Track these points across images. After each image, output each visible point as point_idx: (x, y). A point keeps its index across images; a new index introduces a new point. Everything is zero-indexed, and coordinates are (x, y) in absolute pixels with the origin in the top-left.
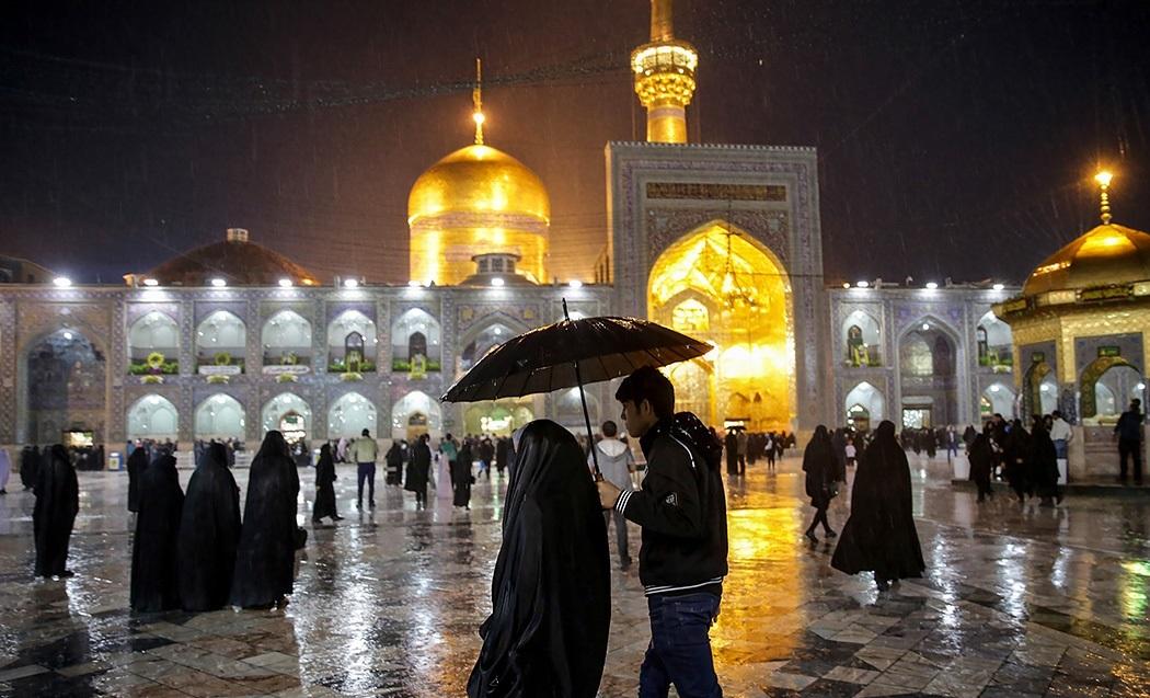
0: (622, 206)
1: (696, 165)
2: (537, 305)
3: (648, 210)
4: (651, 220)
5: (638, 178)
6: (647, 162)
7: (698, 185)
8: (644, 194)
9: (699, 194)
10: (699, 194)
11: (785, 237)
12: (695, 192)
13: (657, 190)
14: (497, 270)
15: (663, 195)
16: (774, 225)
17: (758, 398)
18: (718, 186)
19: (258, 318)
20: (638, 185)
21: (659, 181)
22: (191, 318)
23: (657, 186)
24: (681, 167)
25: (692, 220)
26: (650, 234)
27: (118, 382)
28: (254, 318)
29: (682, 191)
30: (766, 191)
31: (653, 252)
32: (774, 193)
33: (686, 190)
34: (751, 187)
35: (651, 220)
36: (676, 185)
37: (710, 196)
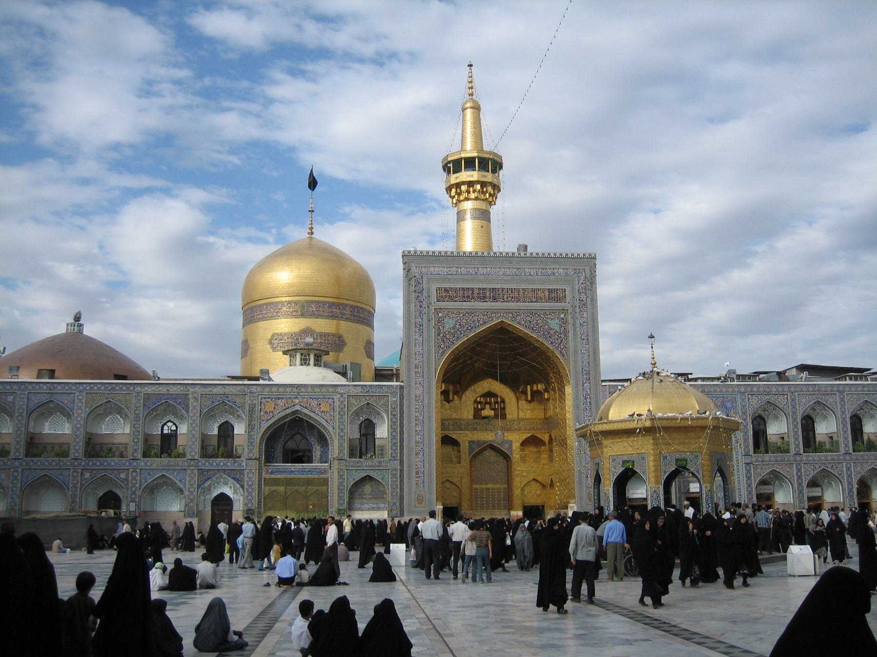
2: (333, 399)
4: (440, 321)
5: (428, 283)
6: (436, 269)
7: (484, 289)
8: (434, 298)
9: (485, 297)
10: (485, 297)
11: (565, 335)
12: (482, 295)
14: (305, 363)
15: (451, 299)
16: (554, 324)
18: (503, 289)
20: (429, 289)
21: (447, 286)
23: (446, 290)
26: (439, 335)
29: (468, 295)
30: (547, 293)
32: (555, 296)
34: (533, 290)
35: (440, 321)
36: (463, 289)
37: (495, 299)
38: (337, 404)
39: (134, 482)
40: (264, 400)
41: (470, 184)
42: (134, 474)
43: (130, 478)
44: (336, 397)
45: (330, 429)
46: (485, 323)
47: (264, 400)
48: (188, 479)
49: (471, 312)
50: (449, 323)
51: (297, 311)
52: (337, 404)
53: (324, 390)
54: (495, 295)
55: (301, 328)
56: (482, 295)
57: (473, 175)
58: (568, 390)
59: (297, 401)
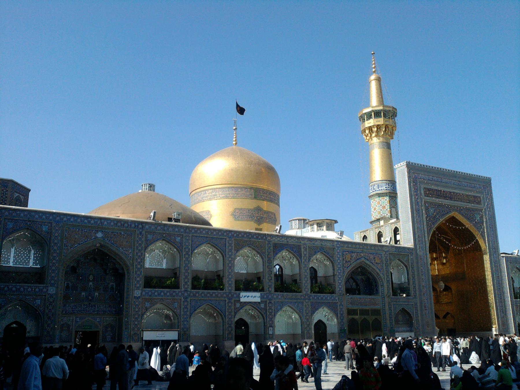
0: (413, 200)
1: (444, 180)
3: (425, 202)
13: (429, 192)
14: (320, 229)
17: (445, 317)
19: (233, 251)
21: (429, 187)
22: (190, 247)
23: (429, 190)
27: (137, 293)
28: (230, 251)
29: (439, 194)
32: (476, 200)
37: (451, 199)
38: (384, 259)
39: (270, 311)
40: (344, 253)
41: (378, 127)
42: (270, 305)
43: (268, 308)
45: (382, 275)
46: (448, 213)
47: (344, 253)
48: (305, 309)
49: (440, 205)
51: (252, 195)
52: (384, 259)
53: (376, 248)
54: (450, 196)
55: (255, 207)
57: (381, 121)
58: (487, 258)
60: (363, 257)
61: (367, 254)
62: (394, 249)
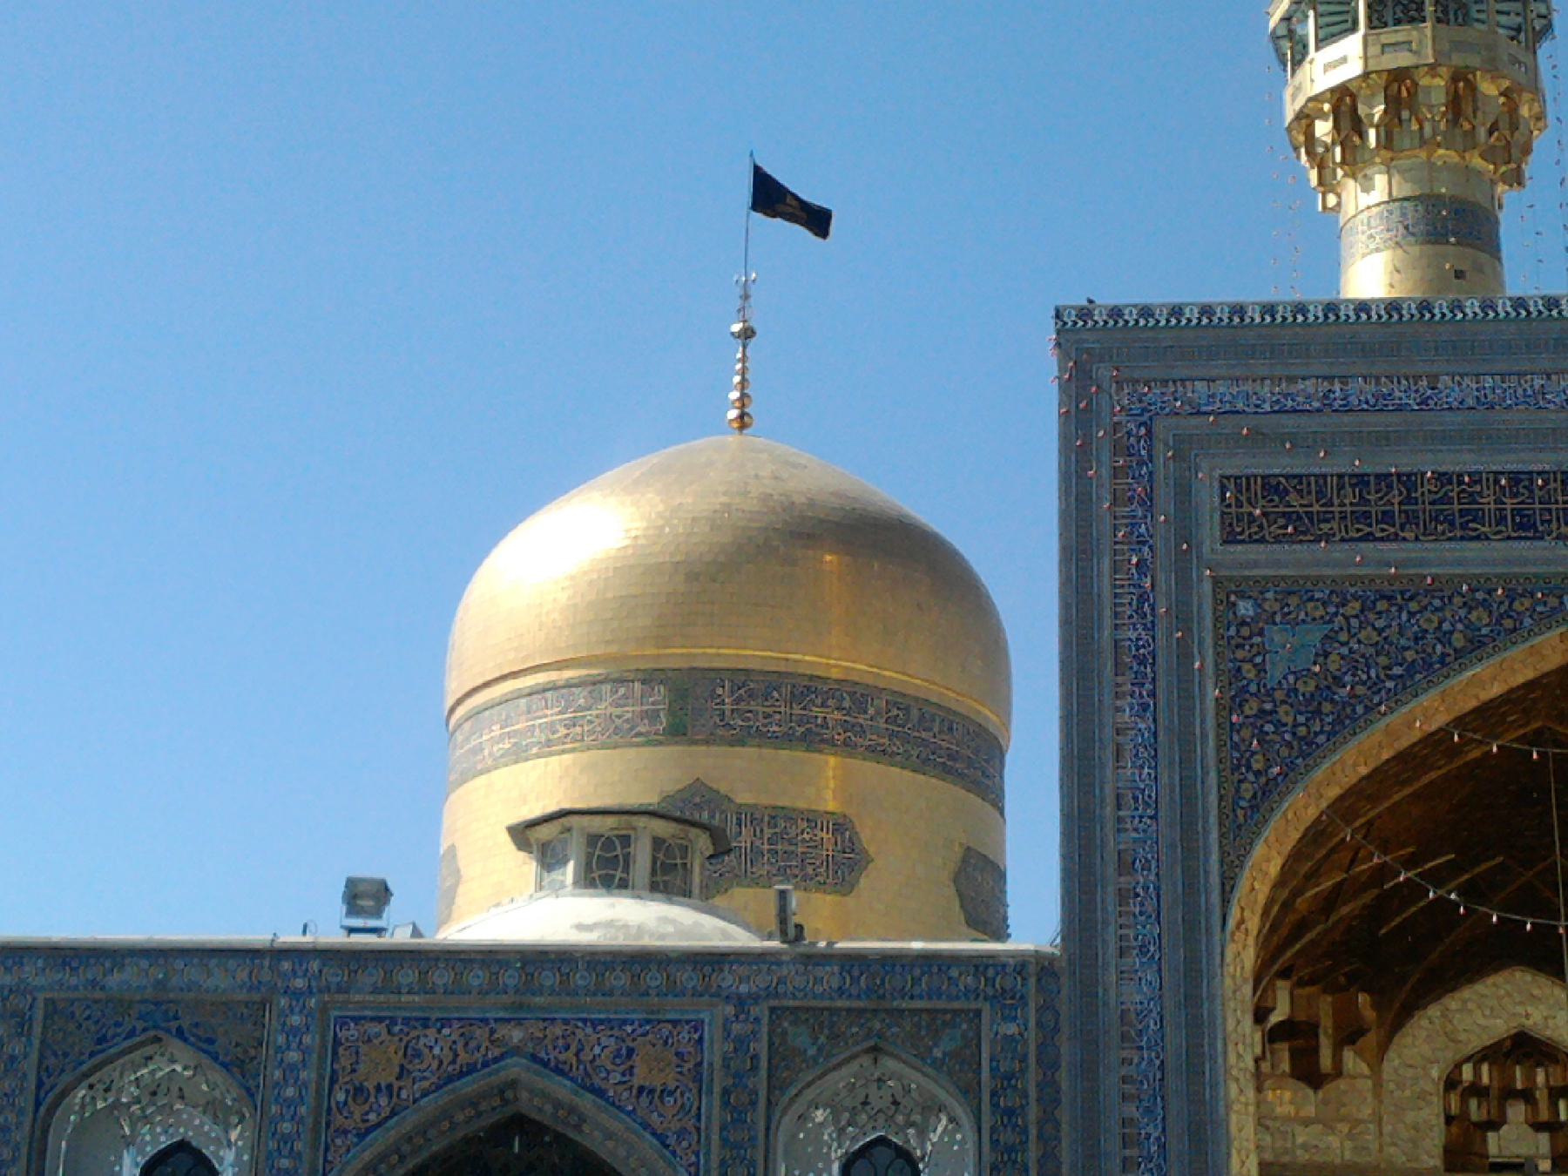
2: (697, 1026)
3: (1227, 590)
8: (1209, 532)
12: (1452, 507)
21: (1280, 465)
23: (1272, 487)
24: (1380, 404)
25: (1445, 638)
26: (1238, 701)
31: (1247, 790)
33: (1409, 500)
36: (1361, 480)
44: (714, 1016)
49: (1397, 595)
50: (1289, 650)
56: (1452, 507)
59: (516, 1035)
60: (516, 1051)
61: (558, 1030)
62: (830, 977)
